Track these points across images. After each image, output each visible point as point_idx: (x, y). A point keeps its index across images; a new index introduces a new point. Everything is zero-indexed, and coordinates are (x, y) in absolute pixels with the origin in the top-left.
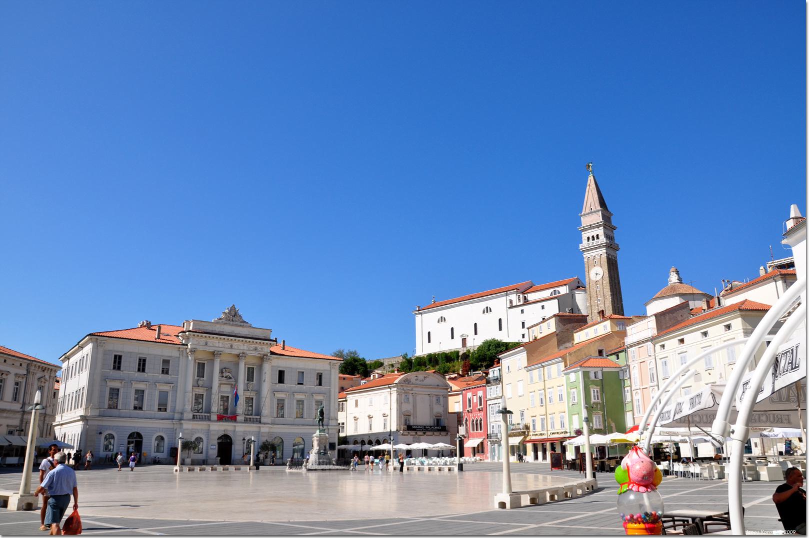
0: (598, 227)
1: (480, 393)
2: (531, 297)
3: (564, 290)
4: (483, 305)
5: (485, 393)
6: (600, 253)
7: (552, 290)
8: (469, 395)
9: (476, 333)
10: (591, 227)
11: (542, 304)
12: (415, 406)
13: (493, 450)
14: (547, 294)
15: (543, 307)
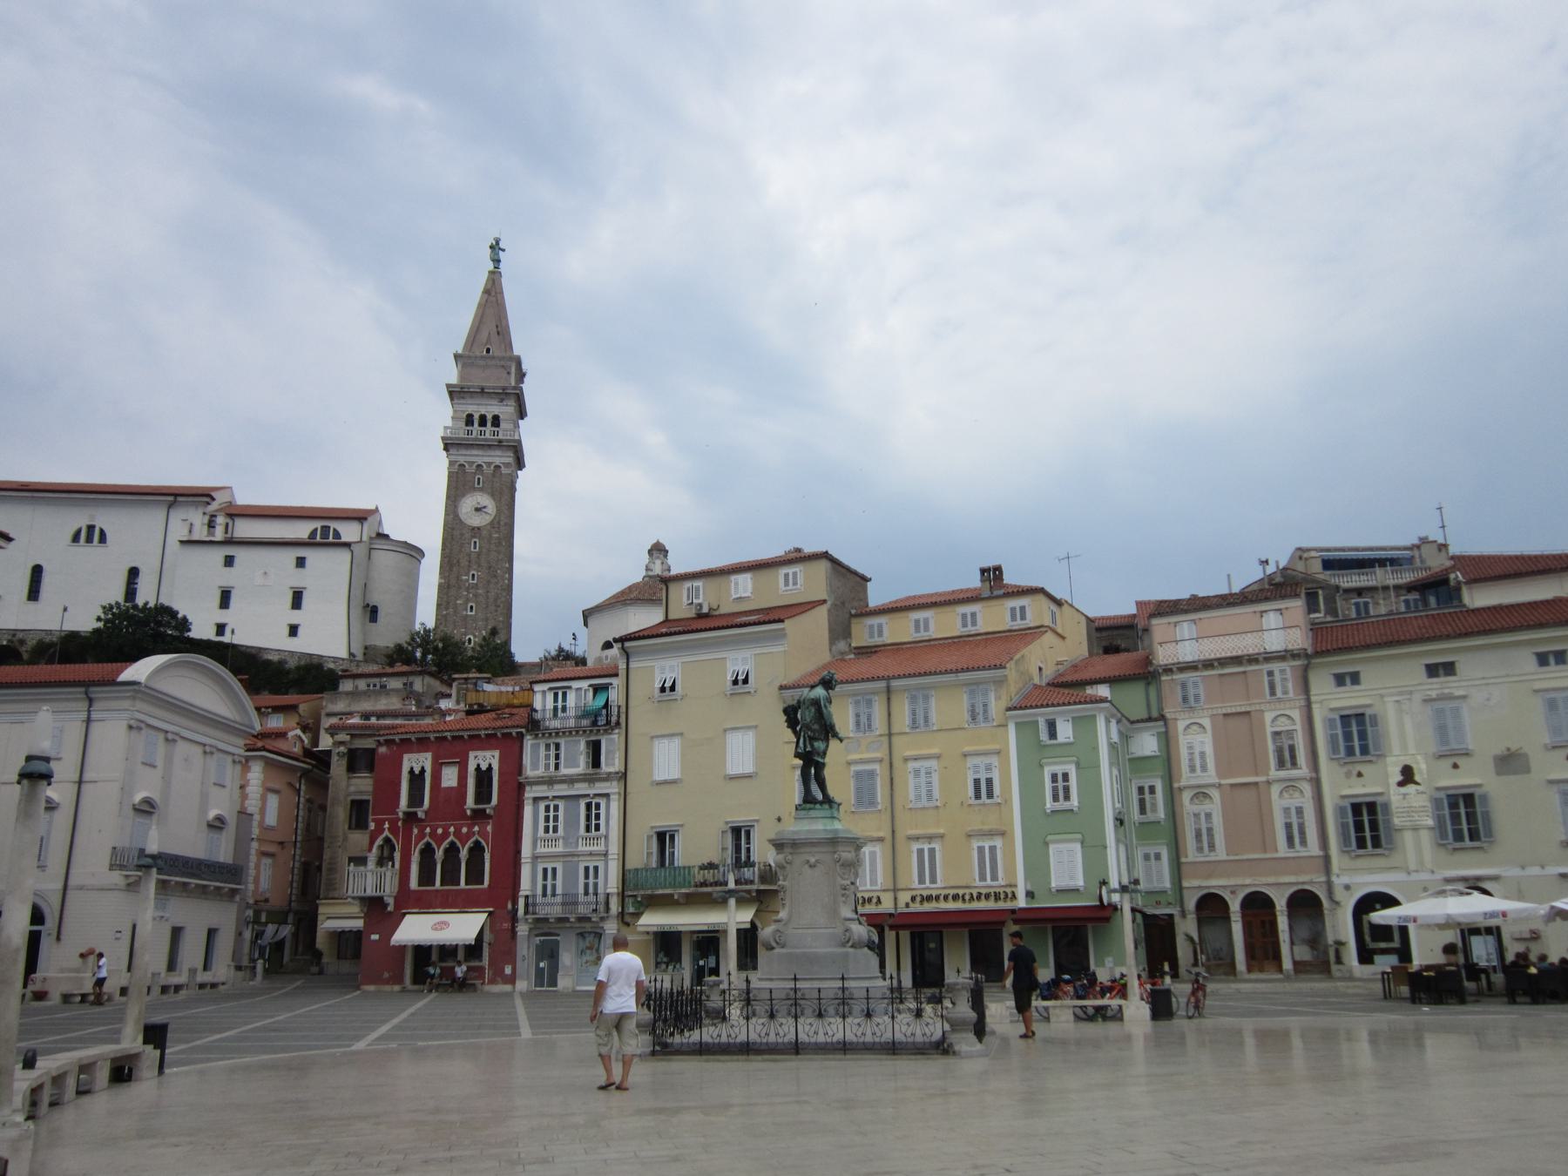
0: (503, 395)
1: (488, 758)
2: (244, 529)
3: (349, 532)
4: (79, 518)
5: (513, 764)
6: (498, 461)
7: (318, 524)
8: (420, 761)
9: (34, 593)
10: (482, 392)
11: (301, 552)
12: (166, 780)
13: (549, 953)
14: (302, 530)
15: (301, 562)
